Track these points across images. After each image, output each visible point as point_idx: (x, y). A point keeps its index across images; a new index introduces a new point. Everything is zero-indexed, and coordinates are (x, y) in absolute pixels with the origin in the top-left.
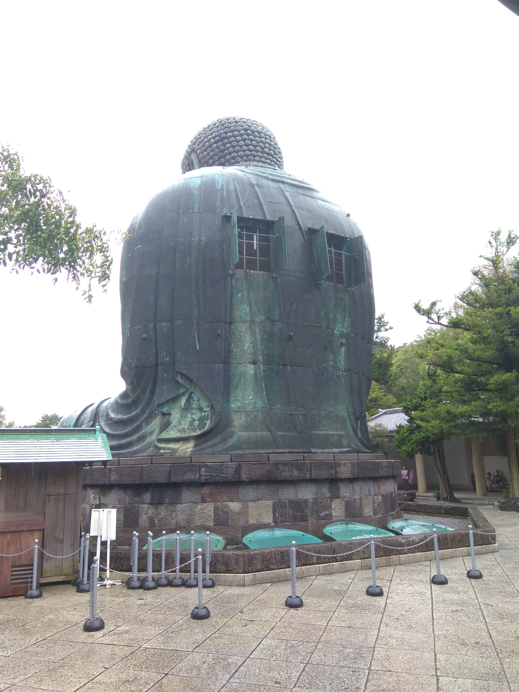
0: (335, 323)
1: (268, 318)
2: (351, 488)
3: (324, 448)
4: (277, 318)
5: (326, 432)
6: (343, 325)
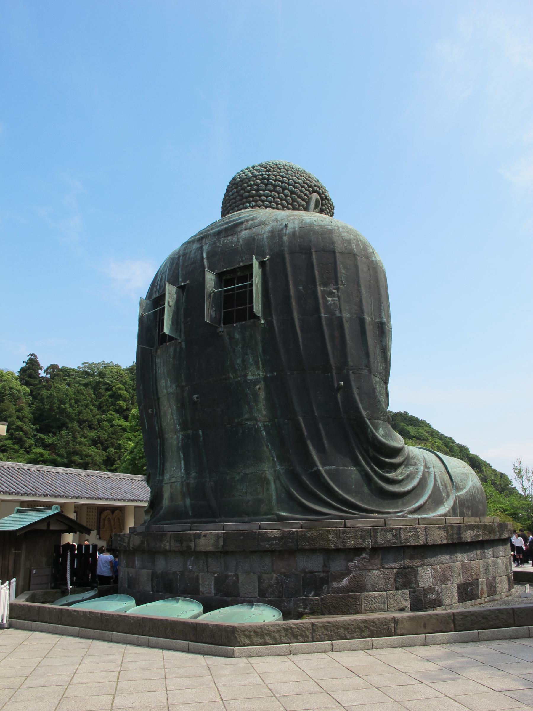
0: (245, 367)
3: (233, 517)
4: (184, 384)
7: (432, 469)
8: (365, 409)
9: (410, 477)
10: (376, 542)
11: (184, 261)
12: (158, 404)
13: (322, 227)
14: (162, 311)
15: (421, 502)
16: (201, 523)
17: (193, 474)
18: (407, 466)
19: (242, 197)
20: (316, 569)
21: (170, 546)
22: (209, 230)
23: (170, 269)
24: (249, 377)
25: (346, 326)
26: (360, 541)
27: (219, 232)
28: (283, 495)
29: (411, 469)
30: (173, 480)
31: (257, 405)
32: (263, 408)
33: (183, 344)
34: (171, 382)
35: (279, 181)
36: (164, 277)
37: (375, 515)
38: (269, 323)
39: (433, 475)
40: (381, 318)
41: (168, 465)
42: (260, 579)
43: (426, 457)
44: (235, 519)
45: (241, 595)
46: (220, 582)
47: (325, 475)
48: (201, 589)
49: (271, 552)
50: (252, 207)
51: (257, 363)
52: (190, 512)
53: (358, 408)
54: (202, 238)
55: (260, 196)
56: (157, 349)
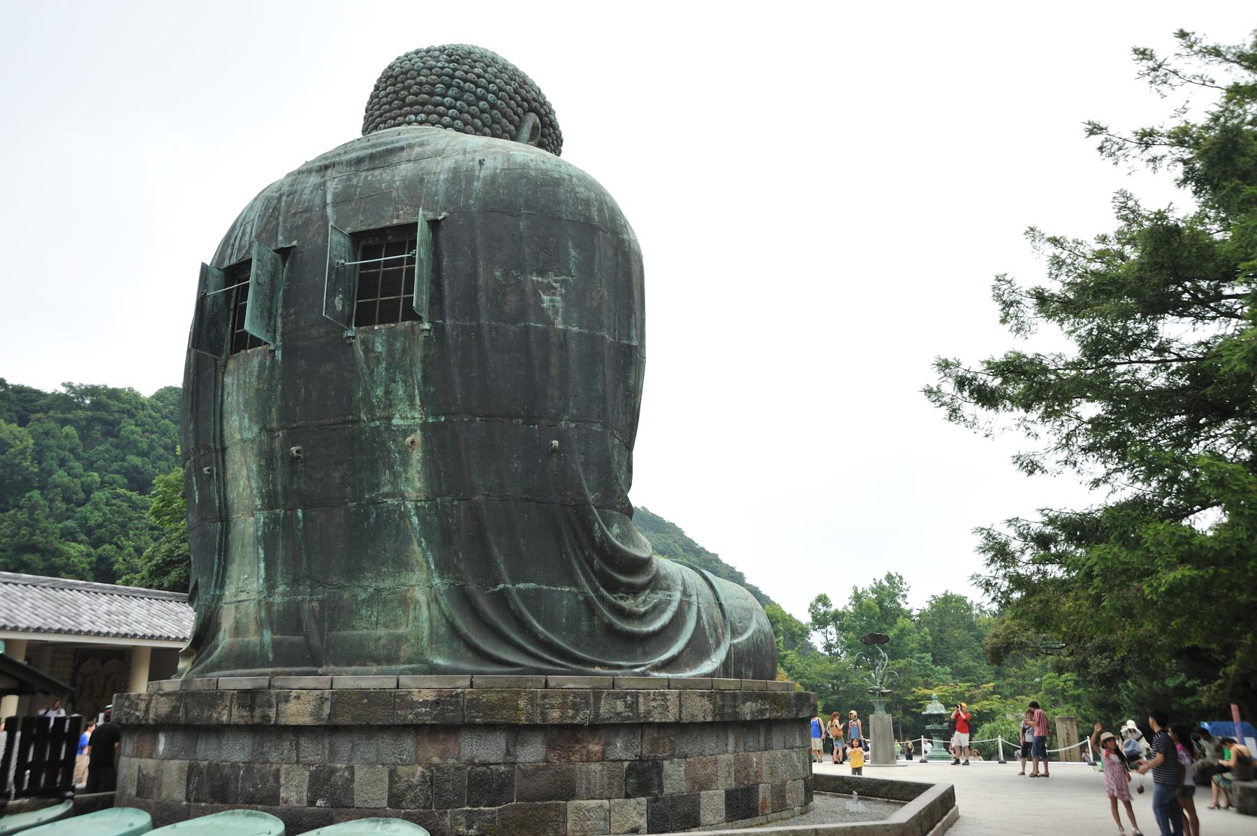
1: (263, 428)
2: (327, 746)
3: (349, 665)
4: (274, 425)
5: (365, 631)
6: (412, 406)
7: (694, 598)
8: (593, 491)
9: (658, 609)
10: (597, 715)
11: (289, 205)
12: (224, 461)
13: (545, 172)
14: (244, 292)
15: (674, 651)
16: (290, 674)
17: (281, 588)
18: (654, 590)
19: (404, 103)
20: (493, 759)
21: (230, 715)
22: (339, 154)
23: (261, 217)
24: (395, 422)
25: (573, 345)
26: (571, 712)
27: (359, 161)
28: (442, 630)
29: (661, 595)
30: (243, 596)
31: (406, 472)
32: (416, 477)
33: (279, 354)
34: (250, 420)
35: (472, 82)
36: (248, 230)
37: (597, 669)
38: (439, 330)
39: (694, 609)
40: (629, 337)
41: (234, 570)
42: (392, 774)
43: (686, 577)
44: (354, 668)
45: (357, 803)
46: (320, 782)
47: (517, 598)
48: (282, 795)
49: (416, 729)
50: (421, 123)
51: (411, 398)
52: (271, 656)
53: (581, 487)
54: (326, 167)
55: (436, 105)
56: (227, 358)
